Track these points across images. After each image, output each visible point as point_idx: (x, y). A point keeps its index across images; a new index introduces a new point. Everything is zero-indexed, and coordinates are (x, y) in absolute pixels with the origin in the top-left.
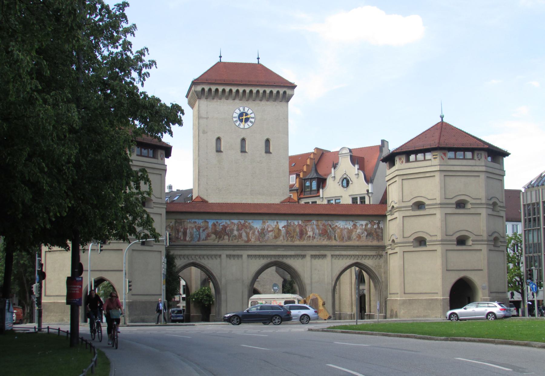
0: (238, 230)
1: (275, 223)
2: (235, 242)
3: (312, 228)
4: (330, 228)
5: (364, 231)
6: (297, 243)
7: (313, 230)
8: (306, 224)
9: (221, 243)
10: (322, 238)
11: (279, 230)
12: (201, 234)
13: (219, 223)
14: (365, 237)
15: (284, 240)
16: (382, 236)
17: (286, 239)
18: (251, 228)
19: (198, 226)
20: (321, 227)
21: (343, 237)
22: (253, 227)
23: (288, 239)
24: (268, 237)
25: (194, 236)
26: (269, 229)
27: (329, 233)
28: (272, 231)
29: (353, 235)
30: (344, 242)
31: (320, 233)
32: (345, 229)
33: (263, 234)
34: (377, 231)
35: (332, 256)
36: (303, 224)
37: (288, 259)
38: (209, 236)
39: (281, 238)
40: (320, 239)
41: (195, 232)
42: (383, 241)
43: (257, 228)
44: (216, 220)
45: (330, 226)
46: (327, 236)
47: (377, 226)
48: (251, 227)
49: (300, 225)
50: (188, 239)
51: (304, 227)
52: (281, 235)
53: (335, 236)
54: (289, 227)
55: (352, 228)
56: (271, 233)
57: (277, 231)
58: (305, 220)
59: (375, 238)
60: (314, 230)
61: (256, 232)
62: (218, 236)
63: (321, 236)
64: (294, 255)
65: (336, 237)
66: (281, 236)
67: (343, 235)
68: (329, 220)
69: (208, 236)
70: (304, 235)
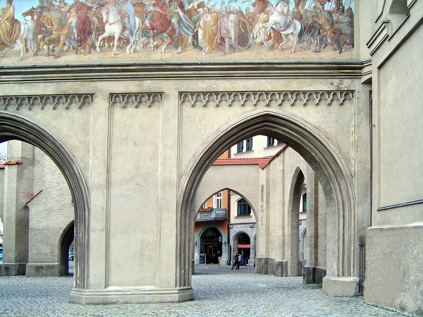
3: (120, 13)
4: (179, 10)
5: (293, 18)
7: (123, 16)
10: (153, 43)
11: (14, 22)
14: (294, 39)
15: (27, 50)
16: (352, 35)
17: (32, 47)
20: (152, 8)
21: (222, 39)
23: (39, 50)
27: (176, 26)
29: (255, 31)
30: (226, 55)
31: (146, 27)
34: (335, 18)
35: (183, 95)
36: (92, 3)
37: (37, 108)
39: (19, 46)
40: (145, 46)
42: (355, 50)
46: (170, 36)
47: (334, 6)
51: (94, 10)
52: (16, 39)
53: (195, 36)
54: (45, 14)
55: (252, 10)
59: (329, 40)
60: (126, 20)
63: (149, 37)
64: (54, 97)
65: (200, 36)
66: (18, 41)
67: (224, 31)
70: (93, 36)
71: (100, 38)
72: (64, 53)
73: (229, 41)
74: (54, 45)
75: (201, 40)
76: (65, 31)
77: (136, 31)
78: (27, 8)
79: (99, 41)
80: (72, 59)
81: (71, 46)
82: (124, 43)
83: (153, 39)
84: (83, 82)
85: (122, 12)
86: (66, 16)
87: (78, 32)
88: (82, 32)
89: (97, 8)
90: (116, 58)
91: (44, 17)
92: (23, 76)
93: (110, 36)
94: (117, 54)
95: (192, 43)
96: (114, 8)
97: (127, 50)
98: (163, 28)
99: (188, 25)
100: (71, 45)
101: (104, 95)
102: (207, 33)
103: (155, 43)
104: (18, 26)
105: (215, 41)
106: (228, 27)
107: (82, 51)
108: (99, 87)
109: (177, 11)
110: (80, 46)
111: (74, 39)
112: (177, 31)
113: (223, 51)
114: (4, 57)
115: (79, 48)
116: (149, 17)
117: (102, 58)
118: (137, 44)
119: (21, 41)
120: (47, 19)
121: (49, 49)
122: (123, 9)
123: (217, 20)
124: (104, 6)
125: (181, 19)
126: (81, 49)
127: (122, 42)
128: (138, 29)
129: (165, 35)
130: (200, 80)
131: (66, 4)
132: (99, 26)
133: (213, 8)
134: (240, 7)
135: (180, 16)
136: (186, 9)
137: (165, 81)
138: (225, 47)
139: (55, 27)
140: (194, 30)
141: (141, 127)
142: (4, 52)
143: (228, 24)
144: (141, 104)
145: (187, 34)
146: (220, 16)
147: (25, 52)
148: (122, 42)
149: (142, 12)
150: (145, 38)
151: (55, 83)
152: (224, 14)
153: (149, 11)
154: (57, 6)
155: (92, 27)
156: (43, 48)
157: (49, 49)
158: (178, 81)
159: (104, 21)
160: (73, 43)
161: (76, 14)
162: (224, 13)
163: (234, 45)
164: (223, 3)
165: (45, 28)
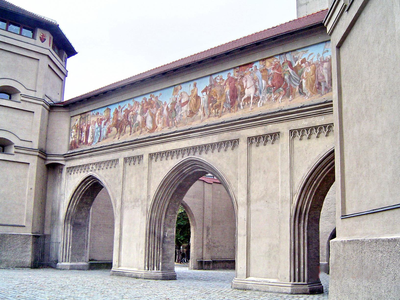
0: (143, 112)
1: (192, 87)
2: (138, 136)
3: (253, 79)
4: (289, 69)
6: (227, 117)
7: (255, 80)
8: (242, 75)
9: (122, 139)
10: (274, 96)
11: (198, 98)
12: (102, 130)
13: (121, 108)
15: (204, 115)
17: (207, 113)
18: (158, 105)
19: (101, 118)
20: (272, 71)
21: (319, 84)
22: (161, 102)
23: (210, 113)
24: (181, 115)
25: (96, 134)
26: (183, 101)
27: (288, 81)
28: (187, 102)
31: (269, 86)
32: (325, 61)
33: (174, 113)
36: (237, 77)
38: (110, 132)
39: (200, 112)
41: (97, 128)
43: (166, 103)
44: (118, 103)
45: (290, 65)
46: (284, 89)
48: (157, 104)
49: (232, 78)
50: (89, 141)
51: (238, 80)
52: (199, 108)
53: (301, 86)
56: (185, 108)
57: (193, 100)
58: (240, 66)
60: (257, 84)
61: (165, 112)
62: (119, 129)
64: (218, 143)
65: (304, 85)
66: (200, 110)
68: (286, 53)
69: (109, 131)
70: (239, 98)
71: (243, 100)
72: (223, 113)
73: (324, 85)
74: (218, 109)
75: (305, 88)
76: (224, 98)
77: (263, 90)
78: (204, 88)
79: (242, 101)
80: (228, 117)
81: (227, 108)
82: (256, 100)
83: (274, 94)
84: (232, 132)
85: (255, 78)
86: (224, 88)
87: (230, 98)
88: (233, 97)
89: (240, 79)
90: (252, 111)
91: (212, 91)
92: (200, 132)
93: (248, 97)
94: (252, 109)
95: (298, 92)
96: (250, 77)
97: (259, 105)
98: (280, 84)
99: (296, 78)
100: (227, 107)
101: (245, 139)
102: (308, 82)
103: (275, 96)
104: (200, 100)
105: (314, 87)
106: (323, 73)
107: (233, 110)
108: (242, 134)
109: (288, 69)
110: (231, 107)
111: (229, 103)
112: (289, 84)
113: (321, 93)
114: (193, 121)
115: (231, 108)
116: (270, 78)
117: (244, 113)
118: (264, 99)
119: (201, 110)
120: (214, 92)
121: (215, 112)
122: (255, 76)
123: (314, 70)
124: (244, 77)
125: (291, 75)
126: (232, 109)
127: (255, 100)
128: (264, 88)
129: (281, 89)
130: (303, 119)
131: (223, 80)
132: (242, 91)
133: (311, 61)
134: (330, 56)
135: (290, 73)
136: (293, 67)
137: (280, 123)
138: (322, 90)
139: (218, 97)
140: (299, 82)
141: (268, 159)
142: (193, 118)
143: (323, 71)
144: (268, 142)
145: (295, 85)
146: (317, 66)
147: (204, 117)
148: (255, 100)
149: (266, 76)
150: (269, 94)
151: (218, 135)
152: (319, 64)
153: (270, 73)
154: (219, 82)
155: (238, 93)
156: (213, 112)
157: (215, 112)
158: (289, 122)
159: (244, 87)
160: (228, 106)
161: (229, 86)
162: (320, 63)
163: (328, 87)
164: (319, 56)
165: (213, 99)
